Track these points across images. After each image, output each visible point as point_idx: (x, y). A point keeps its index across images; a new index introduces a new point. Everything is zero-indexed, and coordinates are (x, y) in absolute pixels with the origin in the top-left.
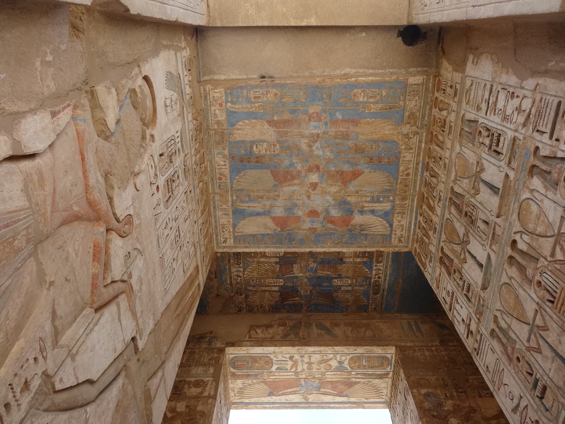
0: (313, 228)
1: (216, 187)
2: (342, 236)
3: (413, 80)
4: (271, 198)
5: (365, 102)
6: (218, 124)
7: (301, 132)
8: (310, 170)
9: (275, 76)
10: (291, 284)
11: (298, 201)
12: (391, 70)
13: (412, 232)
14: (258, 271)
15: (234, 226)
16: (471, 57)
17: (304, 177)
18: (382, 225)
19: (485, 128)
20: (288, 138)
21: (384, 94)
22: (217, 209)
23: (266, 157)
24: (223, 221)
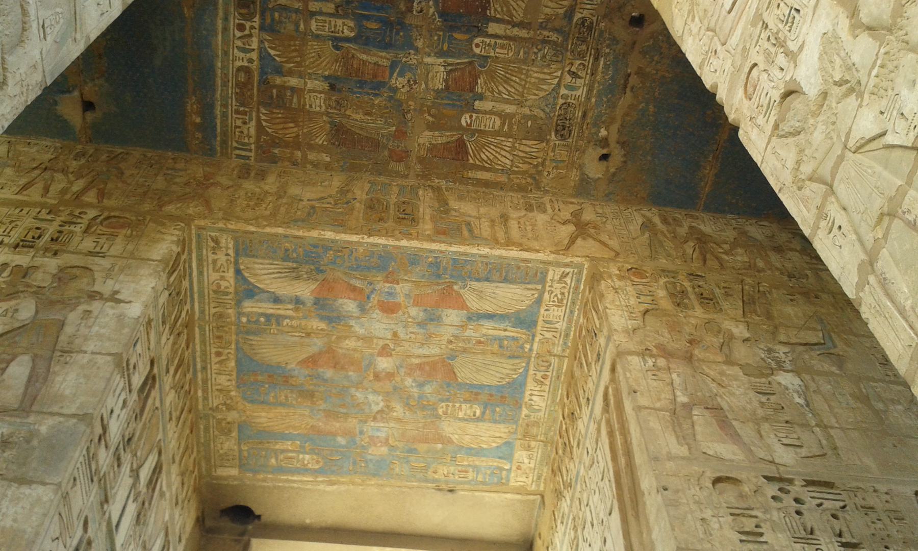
2: (335, 263)
4: (464, 341)
8: (390, 376)
10: (457, 36)
11: (414, 330)
13: (194, 255)
14: (526, 82)
15: (539, 301)
17: (401, 367)
18: (256, 275)
22: (563, 333)
24: (556, 313)
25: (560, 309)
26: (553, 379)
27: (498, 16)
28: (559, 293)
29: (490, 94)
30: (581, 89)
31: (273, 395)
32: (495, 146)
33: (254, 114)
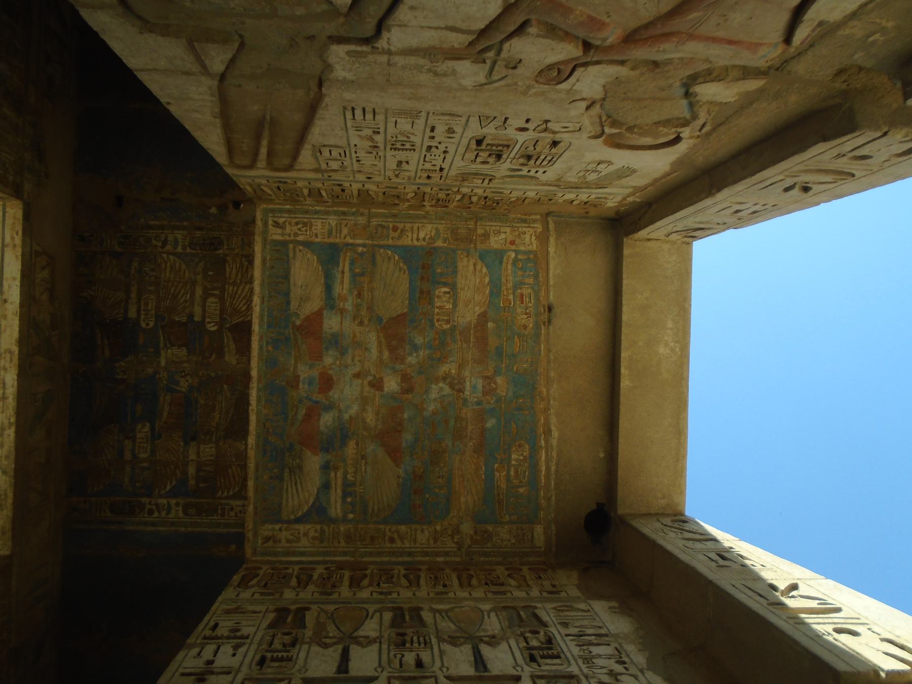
0: (298, 382)
1: (381, 219)
3: (539, 530)
4: (358, 310)
5: (510, 462)
6: (484, 235)
7: (468, 363)
8: (405, 378)
9: (550, 327)
11: (350, 358)
12: (553, 497)
15: (307, 244)
16: (614, 604)
17: (394, 368)
19: (547, 638)
20: (460, 343)
21: (521, 490)
23: (429, 307)
24: (318, 226)
25: (314, 223)
26: (397, 220)
27: (122, 311)
28: (296, 227)
29: (187, 309)
30: (178, 236)
31: (437, 491)
32: (233, 300)
33: (223, 502)
